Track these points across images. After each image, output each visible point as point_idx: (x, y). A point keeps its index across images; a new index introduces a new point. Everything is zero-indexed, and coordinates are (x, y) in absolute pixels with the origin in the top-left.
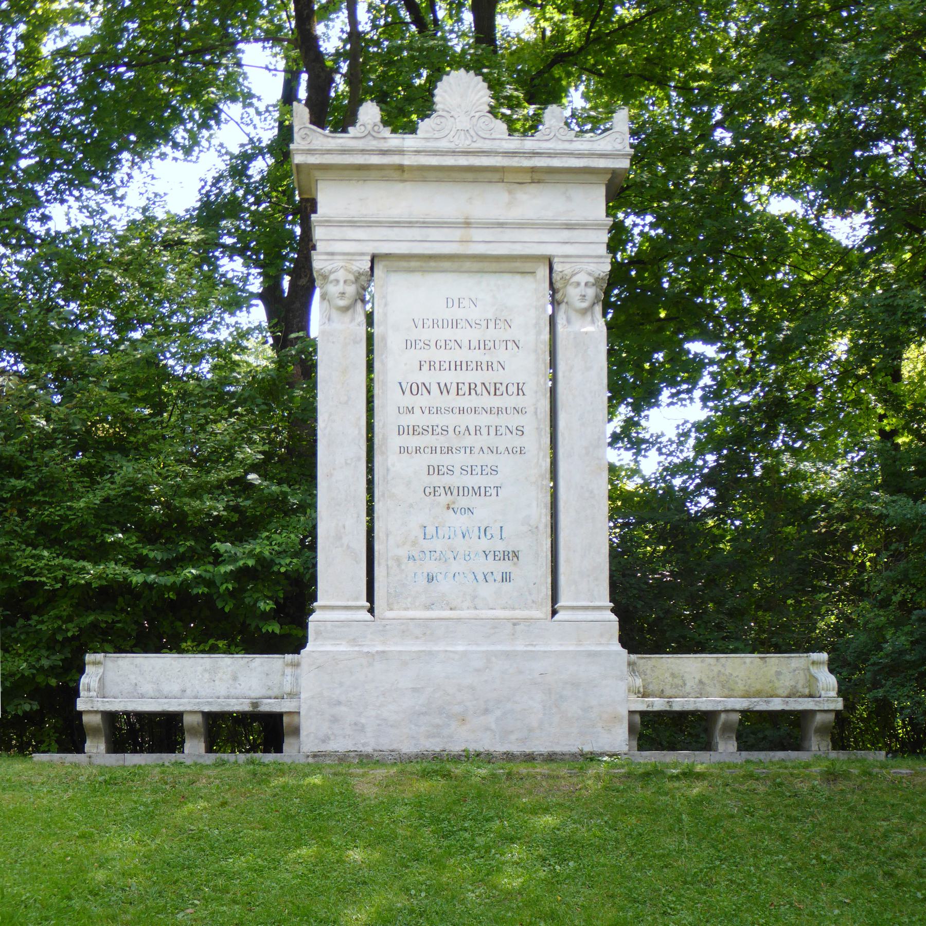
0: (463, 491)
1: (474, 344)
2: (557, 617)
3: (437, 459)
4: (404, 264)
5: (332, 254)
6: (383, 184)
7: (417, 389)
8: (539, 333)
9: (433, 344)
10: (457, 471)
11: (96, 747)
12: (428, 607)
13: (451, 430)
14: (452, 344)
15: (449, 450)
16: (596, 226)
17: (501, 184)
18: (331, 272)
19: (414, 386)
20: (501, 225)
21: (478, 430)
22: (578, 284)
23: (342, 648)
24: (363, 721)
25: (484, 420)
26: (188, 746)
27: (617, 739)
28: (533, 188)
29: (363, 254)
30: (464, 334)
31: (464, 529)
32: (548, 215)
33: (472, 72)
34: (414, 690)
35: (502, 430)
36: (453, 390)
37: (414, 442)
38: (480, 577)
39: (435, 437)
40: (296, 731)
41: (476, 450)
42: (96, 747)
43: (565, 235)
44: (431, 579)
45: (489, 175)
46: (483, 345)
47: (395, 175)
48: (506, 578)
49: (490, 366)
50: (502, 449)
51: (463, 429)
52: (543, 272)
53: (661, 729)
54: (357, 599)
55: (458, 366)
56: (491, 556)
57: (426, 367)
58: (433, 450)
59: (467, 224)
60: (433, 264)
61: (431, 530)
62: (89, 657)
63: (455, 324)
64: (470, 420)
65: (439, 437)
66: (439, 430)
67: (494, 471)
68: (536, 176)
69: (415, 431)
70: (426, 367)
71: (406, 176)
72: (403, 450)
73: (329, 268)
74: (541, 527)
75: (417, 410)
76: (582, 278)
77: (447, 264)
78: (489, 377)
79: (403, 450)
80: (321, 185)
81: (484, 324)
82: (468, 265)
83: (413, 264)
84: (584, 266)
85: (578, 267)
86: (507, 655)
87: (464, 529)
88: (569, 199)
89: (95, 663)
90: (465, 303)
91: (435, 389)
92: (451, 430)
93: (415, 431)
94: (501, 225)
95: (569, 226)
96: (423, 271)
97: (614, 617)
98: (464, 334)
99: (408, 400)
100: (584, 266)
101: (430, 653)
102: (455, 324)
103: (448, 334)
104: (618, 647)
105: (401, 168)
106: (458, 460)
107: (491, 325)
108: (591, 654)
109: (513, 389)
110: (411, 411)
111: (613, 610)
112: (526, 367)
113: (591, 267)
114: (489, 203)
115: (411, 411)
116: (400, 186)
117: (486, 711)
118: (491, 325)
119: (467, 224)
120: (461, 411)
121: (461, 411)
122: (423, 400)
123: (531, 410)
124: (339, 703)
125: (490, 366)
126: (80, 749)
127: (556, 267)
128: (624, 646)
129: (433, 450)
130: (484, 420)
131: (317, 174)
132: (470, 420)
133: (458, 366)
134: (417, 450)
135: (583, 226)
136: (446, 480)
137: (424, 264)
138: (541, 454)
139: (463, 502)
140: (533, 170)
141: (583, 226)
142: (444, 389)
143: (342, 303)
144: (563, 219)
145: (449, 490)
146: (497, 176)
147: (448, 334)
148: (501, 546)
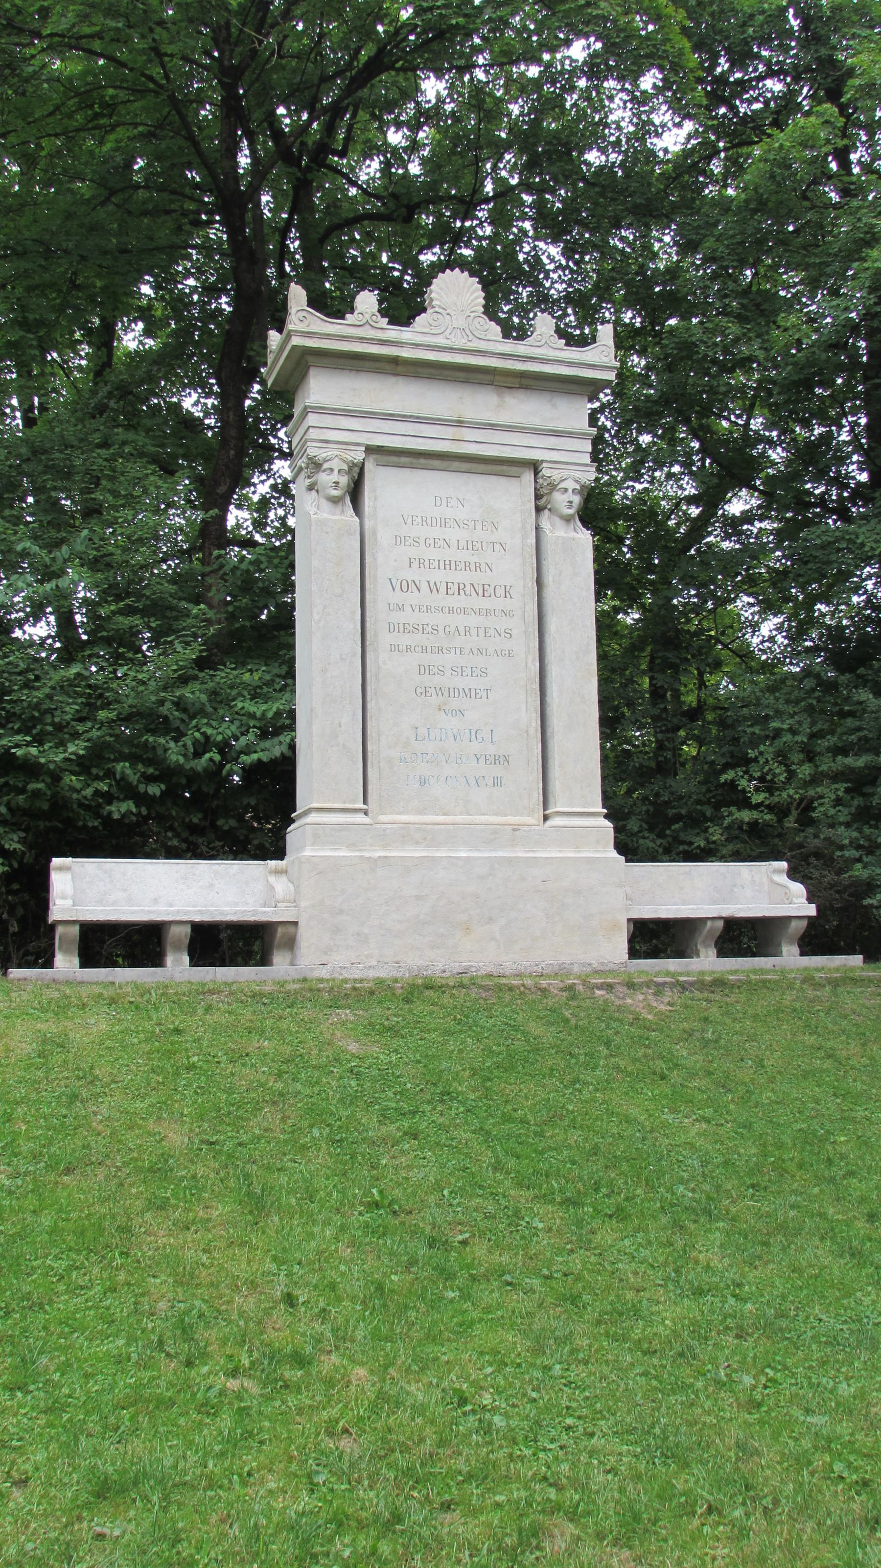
0: (453, 692)
1: (463, 544)
2: (549, 823)
4: (394, 459)
5: (327, 442)
7: (407, 586)
8: (524, 537)
9: (422, 541)
10: (448, 672)
11: (65, 963)
12: (421, 812)
13: (441, 629)
14: (441, 543)
15: (440, 650)
16: (581, 436)
18: (326, 461)
20: (492, 427)
21: (467, 630)
22: (566, 490)
23: (342, 854)
24: (366, 931)
25: (473, 621)
26: (169, 960)
27: (615, 948)
28: (521, 395)
29: (358, 444)
30: (453, 534)
32: (536, 421)
33: (466, 273)
34: (418, 898)
35: (492, 632)
36: (443, 589)
37: (405, 640)
38: (472, 782)
40: (291, 943)
42: (65, 963)
43: (552, 441)
44: (423, 782)
45: (481, 377)
46: (471, 546)
47: (388, 367)
48: (497, 782)
49: (478, 567)
50: (491, 651)
52: (529, 476)
53: (654, 937)
54: (354, 801)
55: (447, 565)
57: (415, 565)
58: (424, 649)
59: (460, 423)
60: (422, 461)
61: (422, 731)
62: (56, 861)
63: (444, 523)
64: (461, 621)
66: (429, 629)
67: (484, 673)
68: (525, 382)
69: (404, 629)
70: (415, 565)
72: (395, 648)
74: (532, 731)
75: (408, 608)
76: (570, 485)
77: (436, 463)
78: (478, 578)
79: (395, 648)
80: (312, 372)
81: (472, 524)
82: (456, 465)
83: (404, 460)
84: (572, 473)
85: (565, 473)
86: (509, 861)
88: (554, 406)
89: (60, 869)
90: (454, 502)
91: (424, 587)
92: (441, 629)
93: (404, 629)
94: (492, 427)
95: (556, 434)
97: (608, 824)
98: (453, 534)
99: (397, 597)
100: (572, 473)
101: (433, 859)
102: (444, 523)
103: (436, 532)
104: (614, 854)
105: (395, 361)
106: (449, 659)
107: (479, 527)
108: (590, 861)
109: (500, 592)
110: (401, 608)
111: (606, 816)
112: (514, 570)
113: (578, 475)
114: (479, 404)
115: (401, 608)
116: (393, 380)
117: (491, 920)
118: (479, 527)
119: (460, 423)
120: (451, 611)
121: (451, 611)
122: (413, 598)
124: (341, 912)
125: (478, 567)
126: (49, 964)
127: (546, 472)
128: (620, 853)
129: (424, 649)
130: (473, 621)
131: (311, 359)
132: (461, 621)
133: (447, 565)
134: (408, 649)
135: (570, 435)
136: (437, 680)
137: (414, 461)
138: (530, 658)
139: (455, 703)
140: (523, 375)
141: (570, 435)
142: (434, 588)
143: (335, 493)
144: (551, 425)
145: (440, 690)
146: (489, 378)
147: (436, 532)
148: (491, 750)
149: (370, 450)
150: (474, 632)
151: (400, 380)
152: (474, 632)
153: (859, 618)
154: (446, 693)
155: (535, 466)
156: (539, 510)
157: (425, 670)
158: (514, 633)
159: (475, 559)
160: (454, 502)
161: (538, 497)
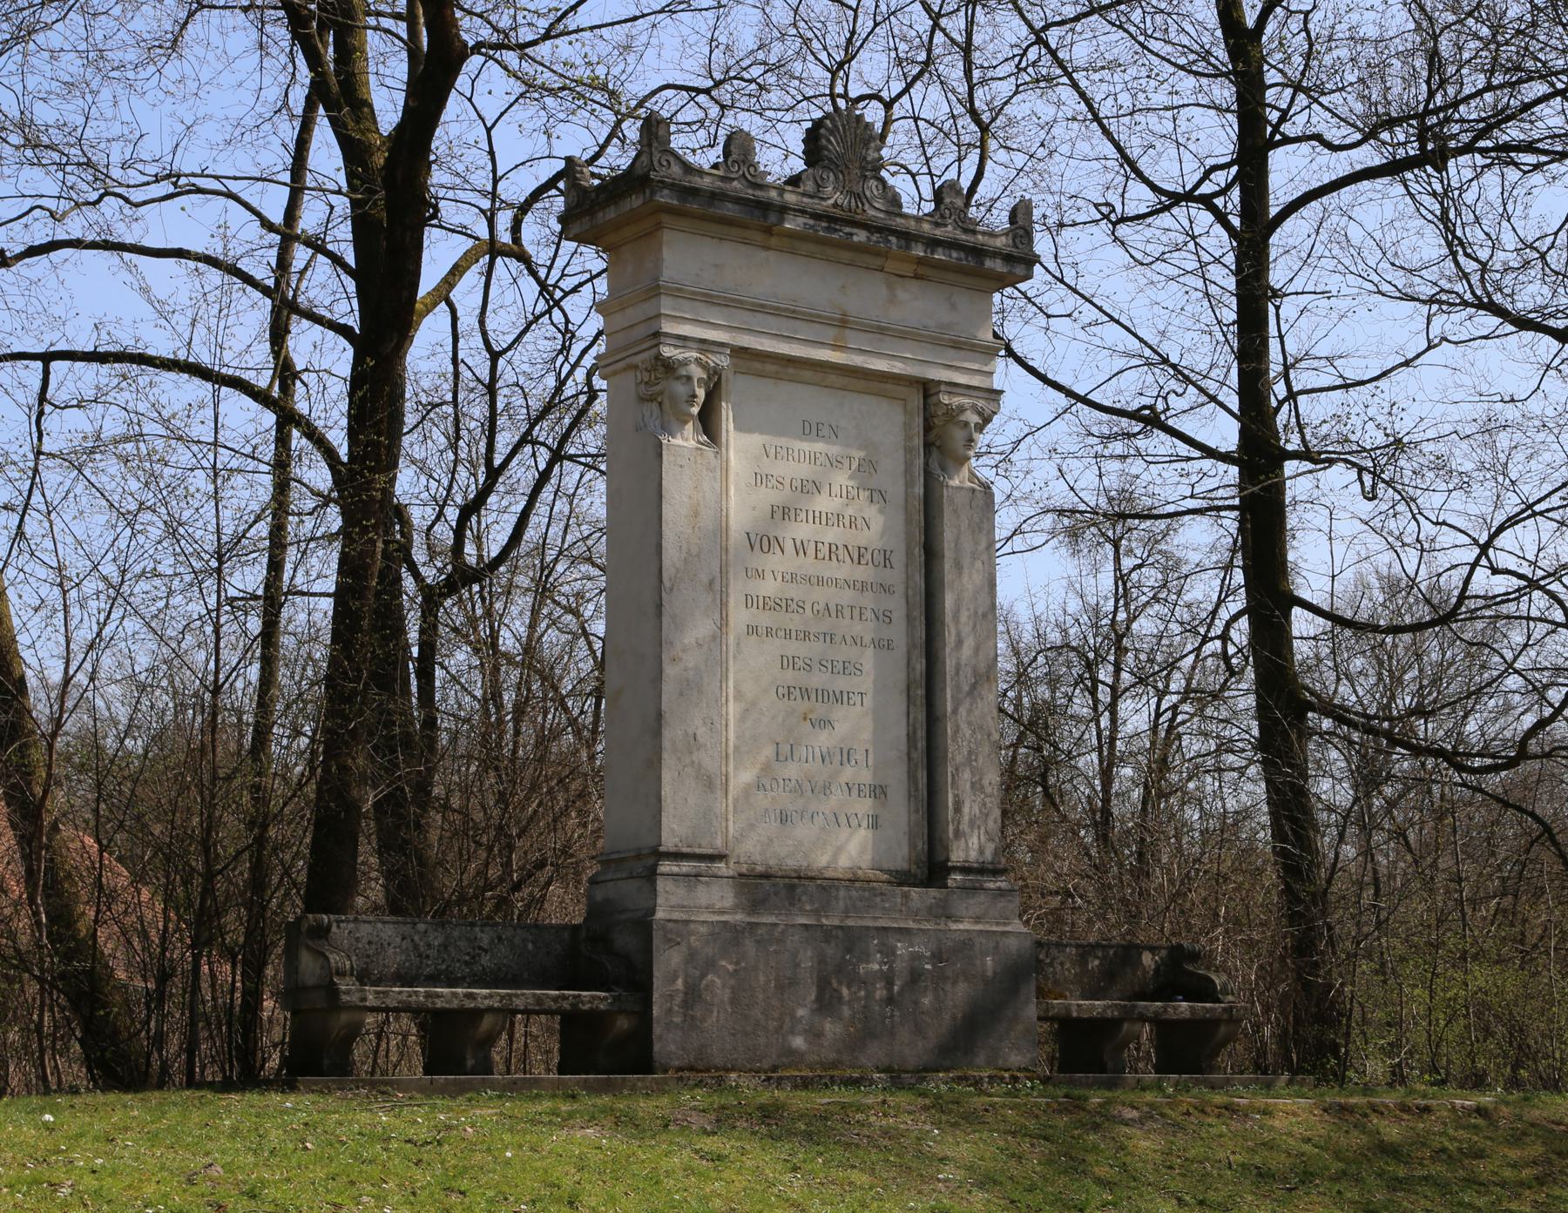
3: (794, 648)
4: (757, 365)
6: (743, 248)
8: (909, 484)
13: (808, 607)
17: (879, 275)
19: (765, 540)
29: (722, 345)
31: (824, 750)
36: (811, 551)
39: (790, 615)
41: (838, 639)
51: (822, 607)
52: (916, 400)
56: (855, 791)
58: (788, 634)
60: (791, 371)
61: (785, 749)
65: (795, 616)
68: (921, 270)
71: (774, 241)
73: (680, 357)
77: (807, 374)
80: (667, 236)
87: (824, 750)
88: (953, 307)
90: (825, 431)
96: (777, 377)
120: (820, 581)
123: (900, 589)
131: (665, 218)
134: (769, 631)
145: (805, 693)
149: (739, 352)
150: (847, 612)
151: (772, 255)
152: (847, 612)
153: (881, 519)
154: (813, 696)
155: (927, 388)
156: (928, 446)
157: (788, 662)
158: (894, 616)
159: (850, 511)
160: (825, 431)
161: (928, 428)
